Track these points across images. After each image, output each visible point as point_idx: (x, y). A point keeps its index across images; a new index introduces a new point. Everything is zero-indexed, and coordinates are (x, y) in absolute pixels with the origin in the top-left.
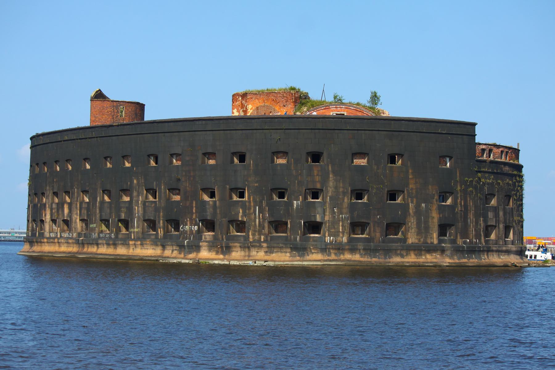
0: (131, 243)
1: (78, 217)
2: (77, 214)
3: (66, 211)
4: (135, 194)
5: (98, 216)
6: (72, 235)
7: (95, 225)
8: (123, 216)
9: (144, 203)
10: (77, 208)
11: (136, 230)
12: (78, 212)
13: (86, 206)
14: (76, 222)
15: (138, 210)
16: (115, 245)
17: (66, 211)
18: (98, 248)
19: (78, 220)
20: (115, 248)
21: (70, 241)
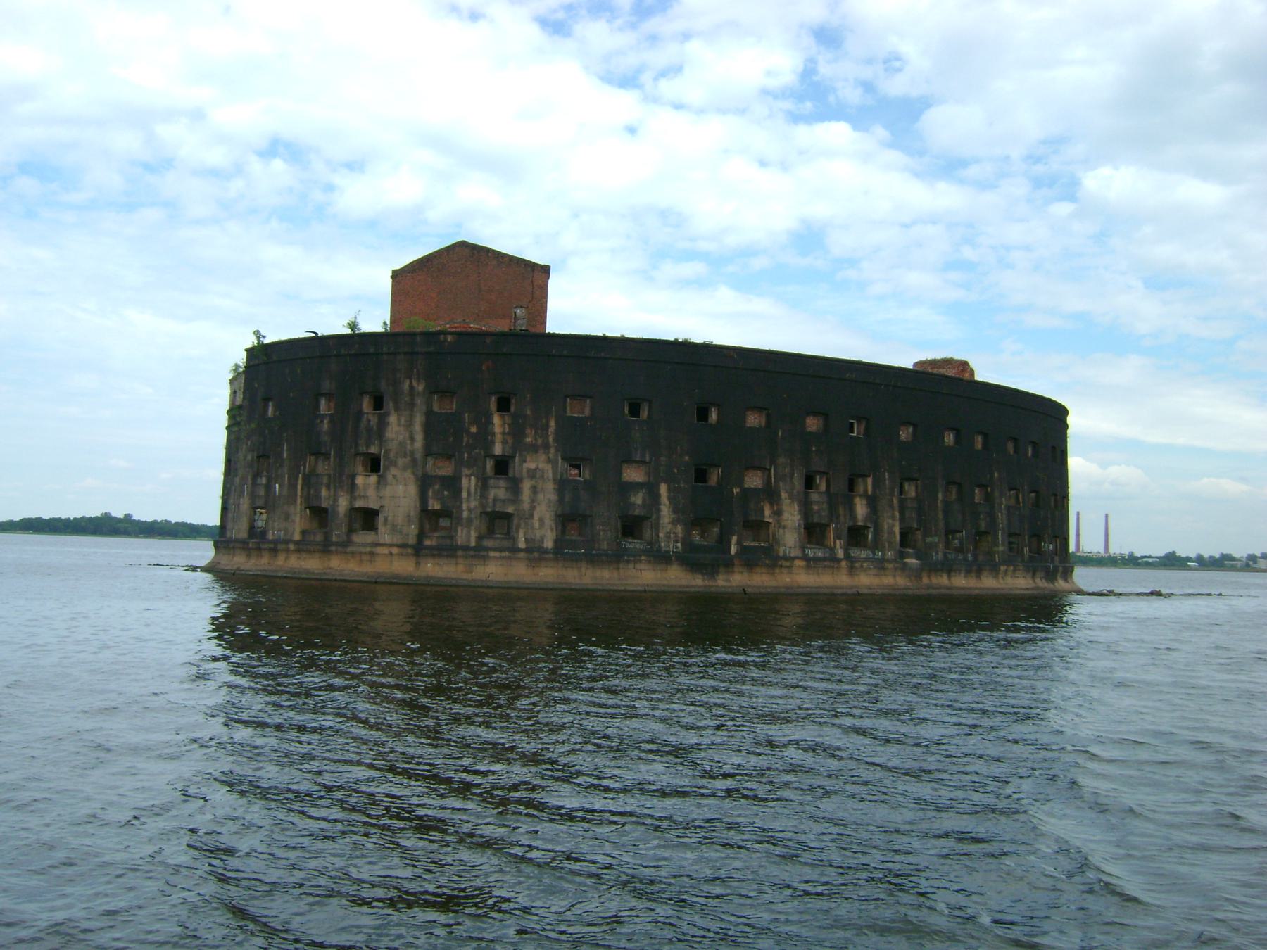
0: (1003, 568)
1: (897, 524)
2: (893, 518)
3: (861, 509)
4: (997, 494)
5: (941, 524)
6: (883, 554)
7: (936, 539)
8: (983, 526)
9: (1008, 508)
10: (892, 506)
11: (1001, 548)
12: (897, 514)
13: (915, 505)
14: (891, 532)
15: (1001, 517)
16: (979, 573)
17: (861, 509)
18: (949, 577)
19: (897, 530)
20: (978, 577)
21: (890, 566)
